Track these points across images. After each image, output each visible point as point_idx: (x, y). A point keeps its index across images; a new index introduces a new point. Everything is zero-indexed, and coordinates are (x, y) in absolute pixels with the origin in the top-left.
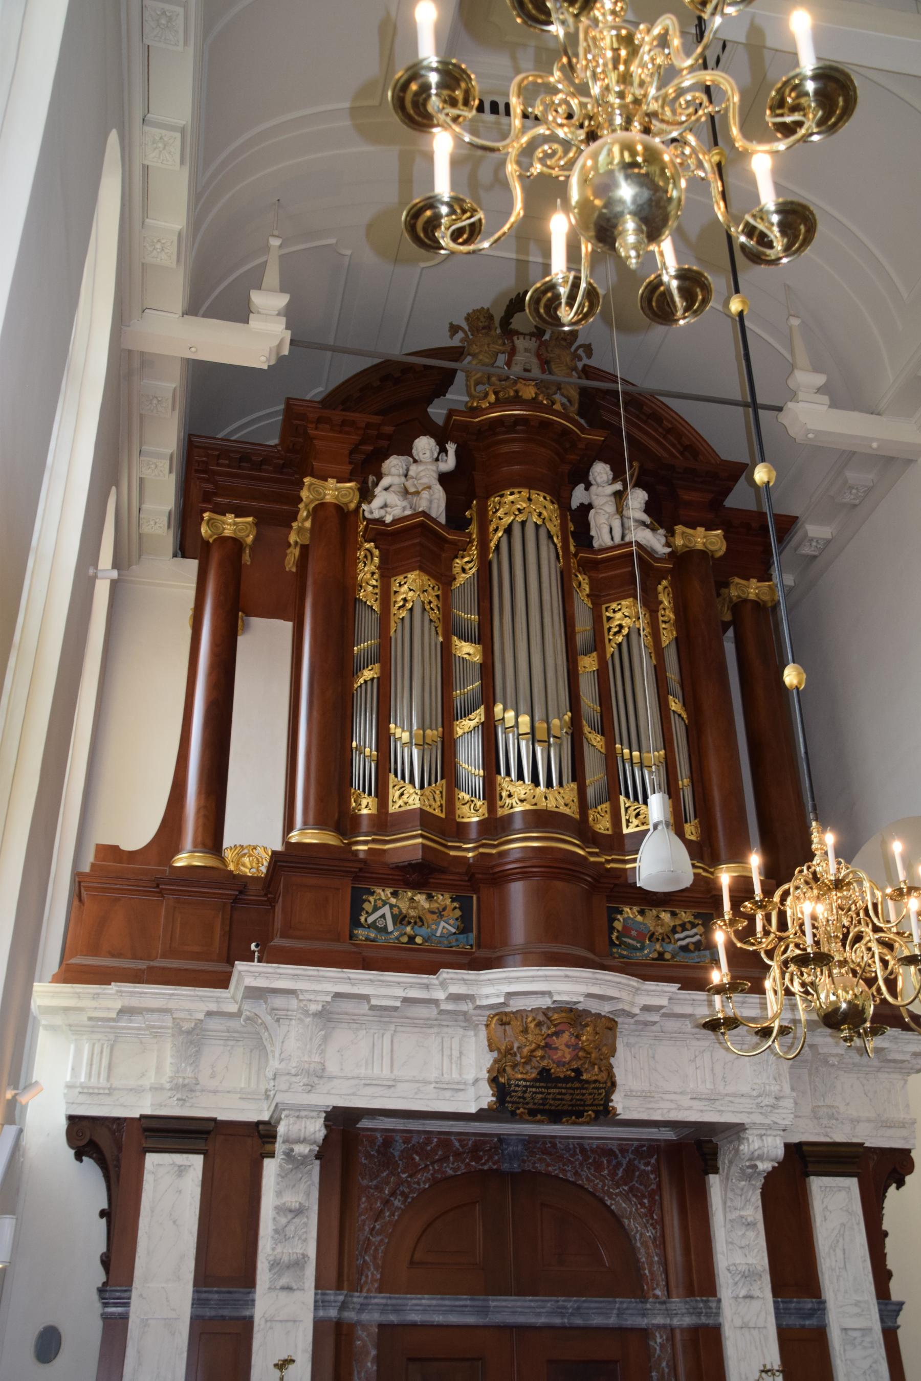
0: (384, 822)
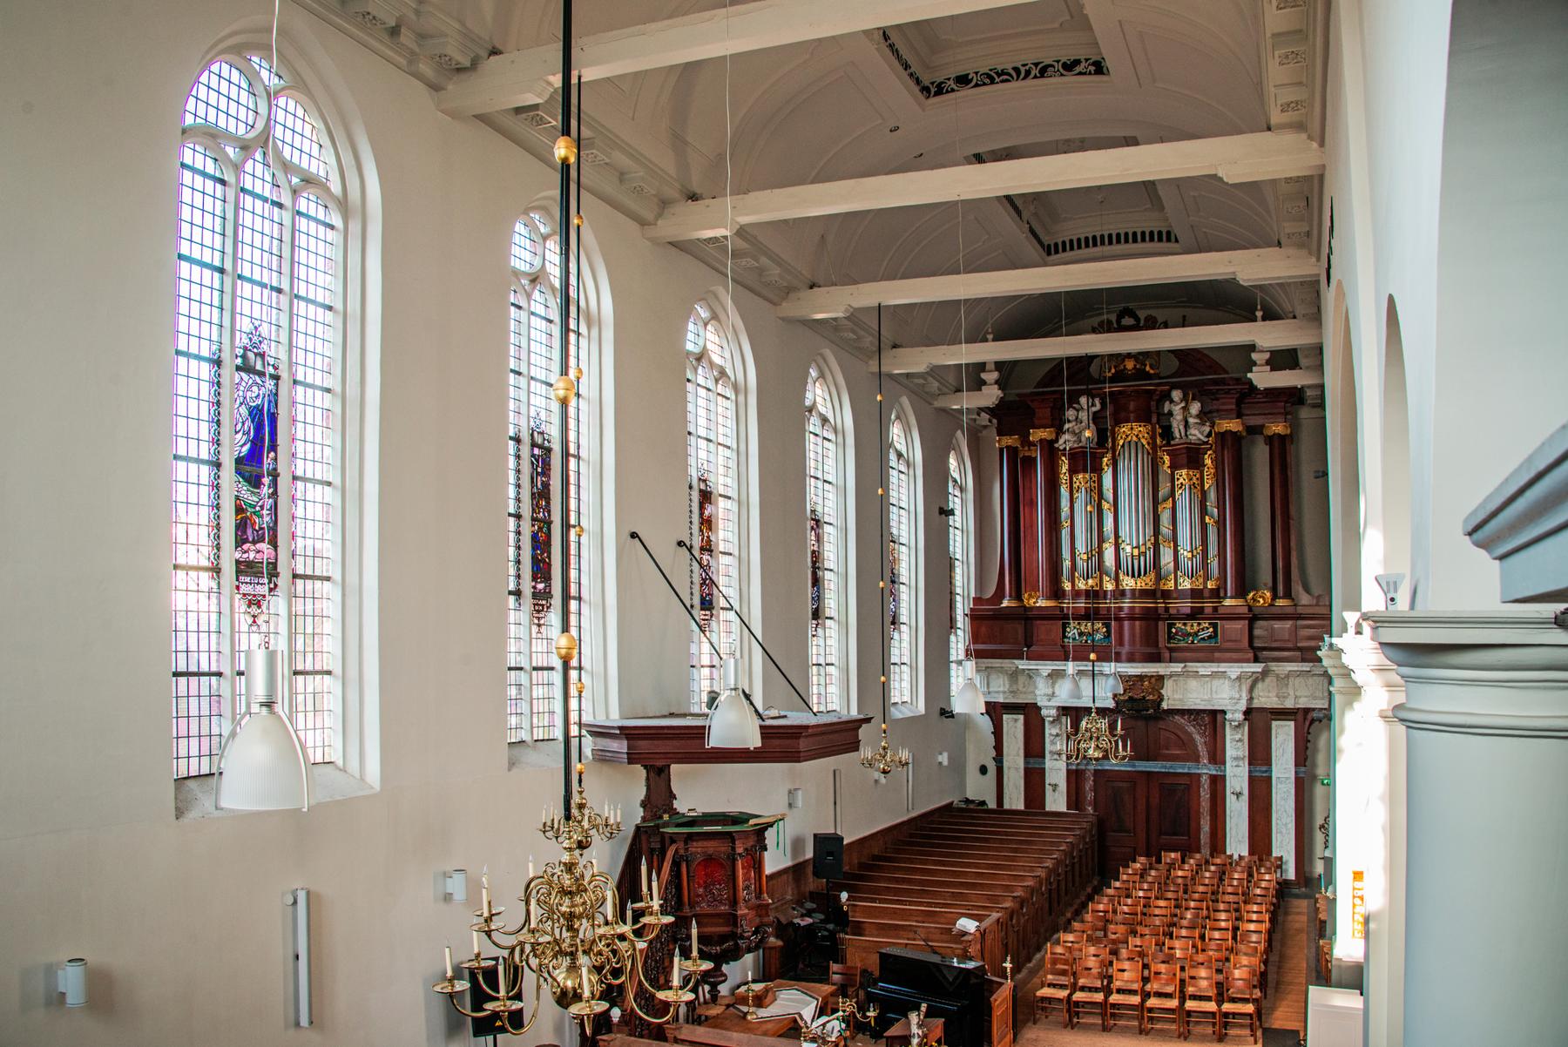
0: (1077, 594)
